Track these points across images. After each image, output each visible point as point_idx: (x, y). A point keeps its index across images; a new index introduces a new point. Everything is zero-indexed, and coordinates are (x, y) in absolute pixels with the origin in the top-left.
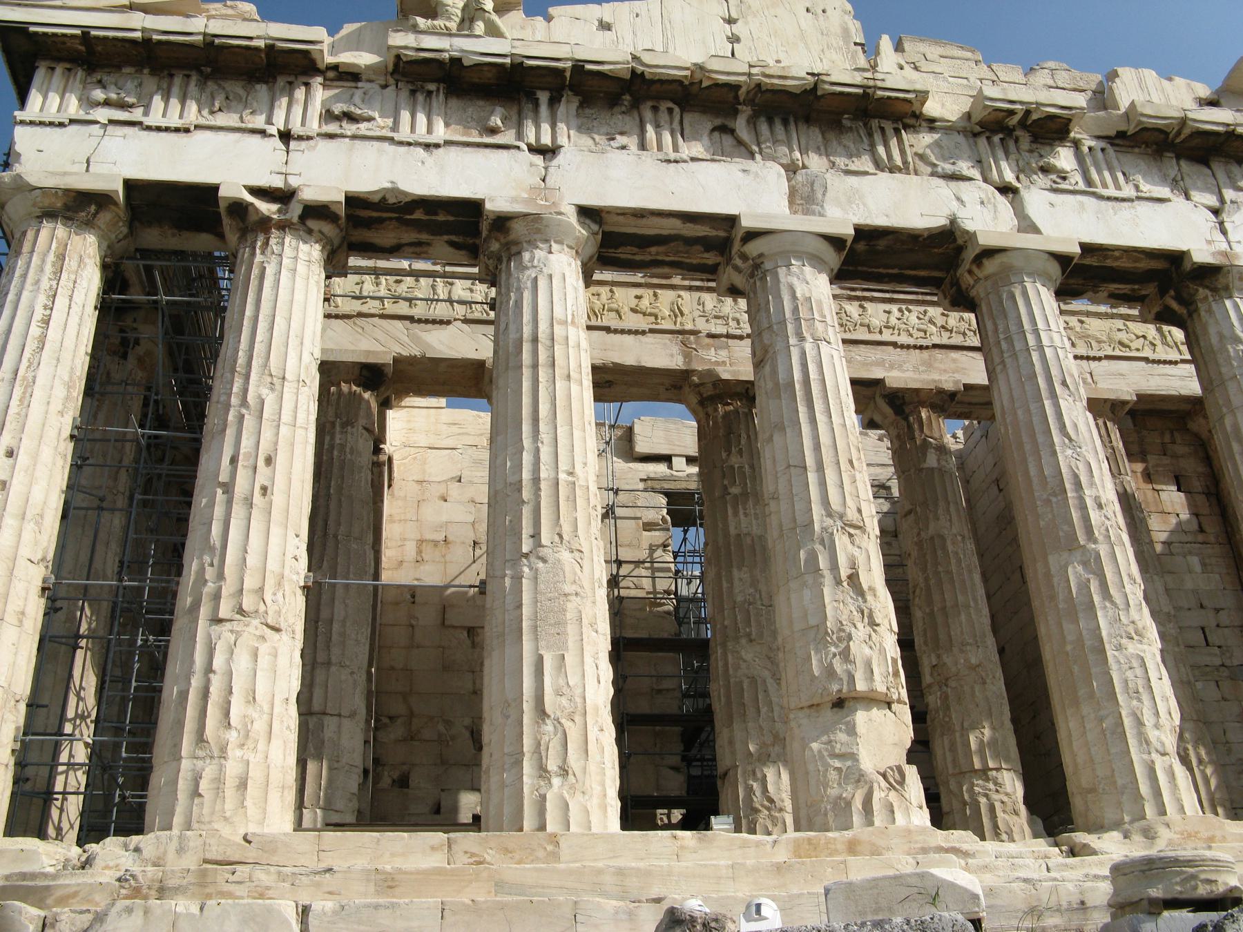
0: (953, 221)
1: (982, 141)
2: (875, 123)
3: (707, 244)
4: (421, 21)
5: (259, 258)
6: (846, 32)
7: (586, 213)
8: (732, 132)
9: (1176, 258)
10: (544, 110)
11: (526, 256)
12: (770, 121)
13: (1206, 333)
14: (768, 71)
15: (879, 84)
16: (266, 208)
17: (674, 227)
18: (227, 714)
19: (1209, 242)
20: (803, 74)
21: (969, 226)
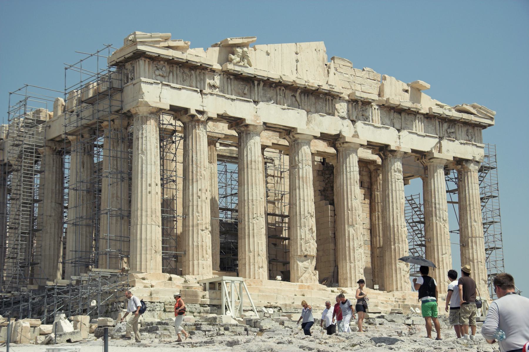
0: (340, 132)
1: (350, 105)
2: (328, 97)
3: (283, 129)
4: (233, 57)
5: (197, 131)
6: (324, 59)
7: (265, 123)
8: (295, 97)
9: (387, 146)
10: (256, 87)
11: (252, 135)
12: (304, 95)
13: (388, 166)
14: (310, 84)
15: (333, 90)
16: (199, 116)
17: (282, 127)
18: (207, 251)
19: (396, 142)
20: (317, 86)
21: (344, 134)
